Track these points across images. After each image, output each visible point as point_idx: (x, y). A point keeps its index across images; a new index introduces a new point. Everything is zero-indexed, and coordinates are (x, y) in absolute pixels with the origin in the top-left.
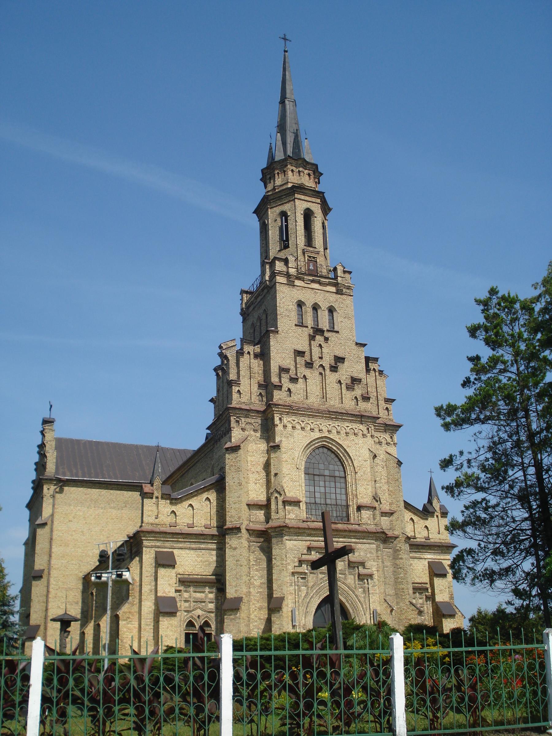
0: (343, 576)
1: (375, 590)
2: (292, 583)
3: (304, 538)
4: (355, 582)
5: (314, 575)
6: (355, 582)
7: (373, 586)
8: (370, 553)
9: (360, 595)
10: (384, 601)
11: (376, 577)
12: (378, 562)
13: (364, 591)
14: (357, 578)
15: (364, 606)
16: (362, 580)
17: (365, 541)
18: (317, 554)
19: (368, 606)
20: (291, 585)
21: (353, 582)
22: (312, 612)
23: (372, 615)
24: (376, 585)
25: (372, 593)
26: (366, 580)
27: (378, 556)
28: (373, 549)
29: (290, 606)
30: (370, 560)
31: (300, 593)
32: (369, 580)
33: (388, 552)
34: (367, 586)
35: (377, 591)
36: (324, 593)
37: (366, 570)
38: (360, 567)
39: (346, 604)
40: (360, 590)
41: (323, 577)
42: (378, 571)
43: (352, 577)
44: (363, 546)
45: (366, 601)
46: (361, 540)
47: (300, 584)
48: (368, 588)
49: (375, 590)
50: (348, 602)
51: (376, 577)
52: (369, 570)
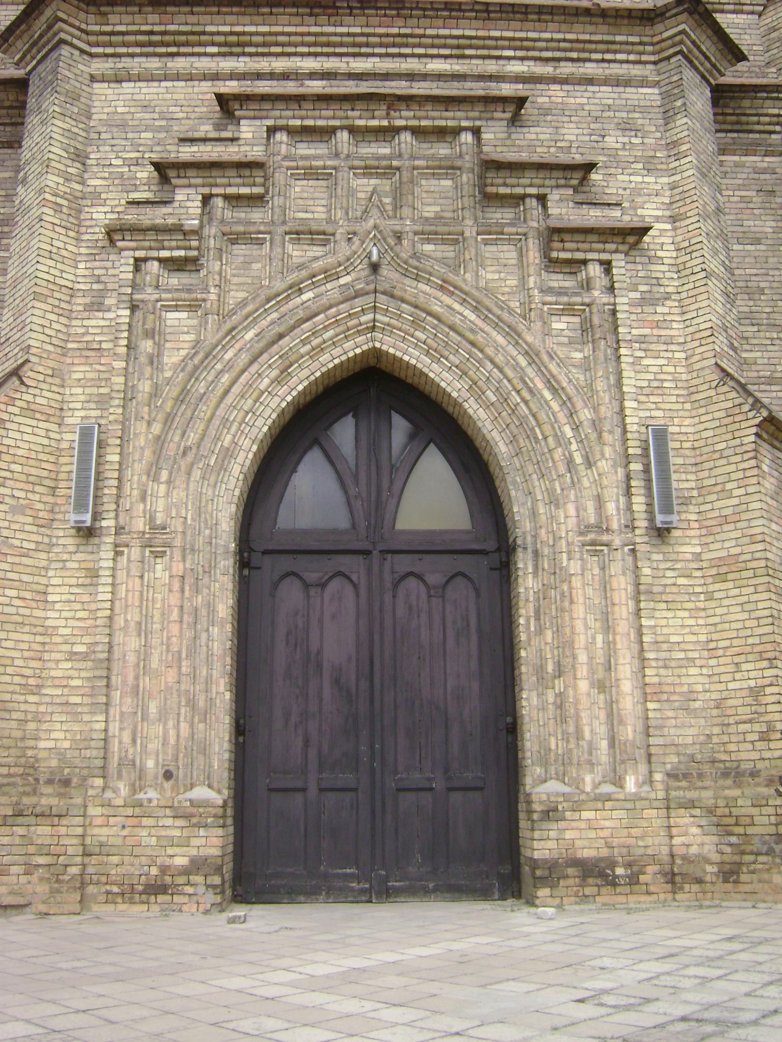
0: (448, 252)
1: (657, 325)
2: (102, 294)
3: (204, 64)
4: (523, 280)
5: (255, 251)
6: (523, 280)
7: (649, 300)
8: (626, 127)
9: (561, 352)
10: (716, 376)
11: (668, 254)
12: (673, 172)
13: (586, 328)
14: (534, 255)
15: (585, 414)
16: (575, 265)
17: (590, 69)
18: (281, 137)
19: (607, 411)
20: (97, 306)
21: (513, 282)
22: (228, 454)
23: (636, 467)
24: (668, 296)
25: (642, 340)
26: (595, 270)
27: (675, 144)
28: (644, 110)
29: (74, 419)
30: (625, 166)
31: (147, 346)
32: (619, 263)
33: (764, 171)
34: (606, 299)
35: (676, 329)
36: (320, 349)
37: (595, 212)
38: (554, 196)
39: (472, 408)
40: (558, 324)
41: (316, 259)
42: (674, 219)
43: (509, 254)
44: (580, 97)
45: (600, 385)
46: (566, 69)
47: (149, 295)
48: (614, 312)
49: (657, 325)
50: (478, 396)
51: (668, 254)
52: (617, 213)
